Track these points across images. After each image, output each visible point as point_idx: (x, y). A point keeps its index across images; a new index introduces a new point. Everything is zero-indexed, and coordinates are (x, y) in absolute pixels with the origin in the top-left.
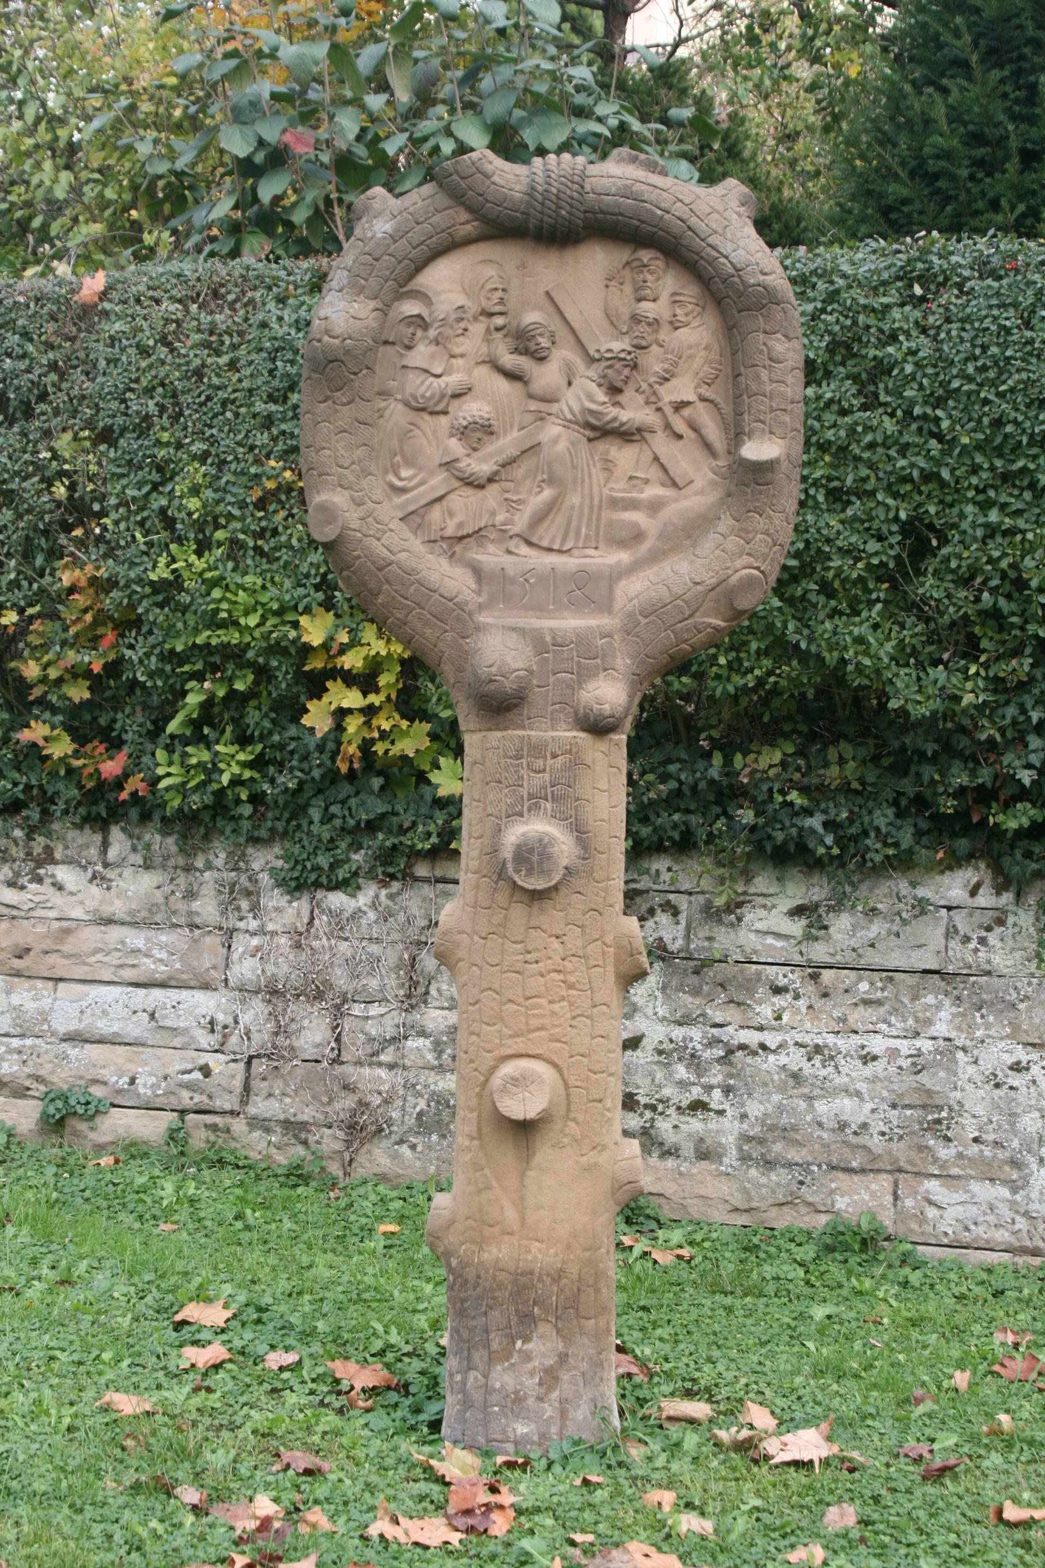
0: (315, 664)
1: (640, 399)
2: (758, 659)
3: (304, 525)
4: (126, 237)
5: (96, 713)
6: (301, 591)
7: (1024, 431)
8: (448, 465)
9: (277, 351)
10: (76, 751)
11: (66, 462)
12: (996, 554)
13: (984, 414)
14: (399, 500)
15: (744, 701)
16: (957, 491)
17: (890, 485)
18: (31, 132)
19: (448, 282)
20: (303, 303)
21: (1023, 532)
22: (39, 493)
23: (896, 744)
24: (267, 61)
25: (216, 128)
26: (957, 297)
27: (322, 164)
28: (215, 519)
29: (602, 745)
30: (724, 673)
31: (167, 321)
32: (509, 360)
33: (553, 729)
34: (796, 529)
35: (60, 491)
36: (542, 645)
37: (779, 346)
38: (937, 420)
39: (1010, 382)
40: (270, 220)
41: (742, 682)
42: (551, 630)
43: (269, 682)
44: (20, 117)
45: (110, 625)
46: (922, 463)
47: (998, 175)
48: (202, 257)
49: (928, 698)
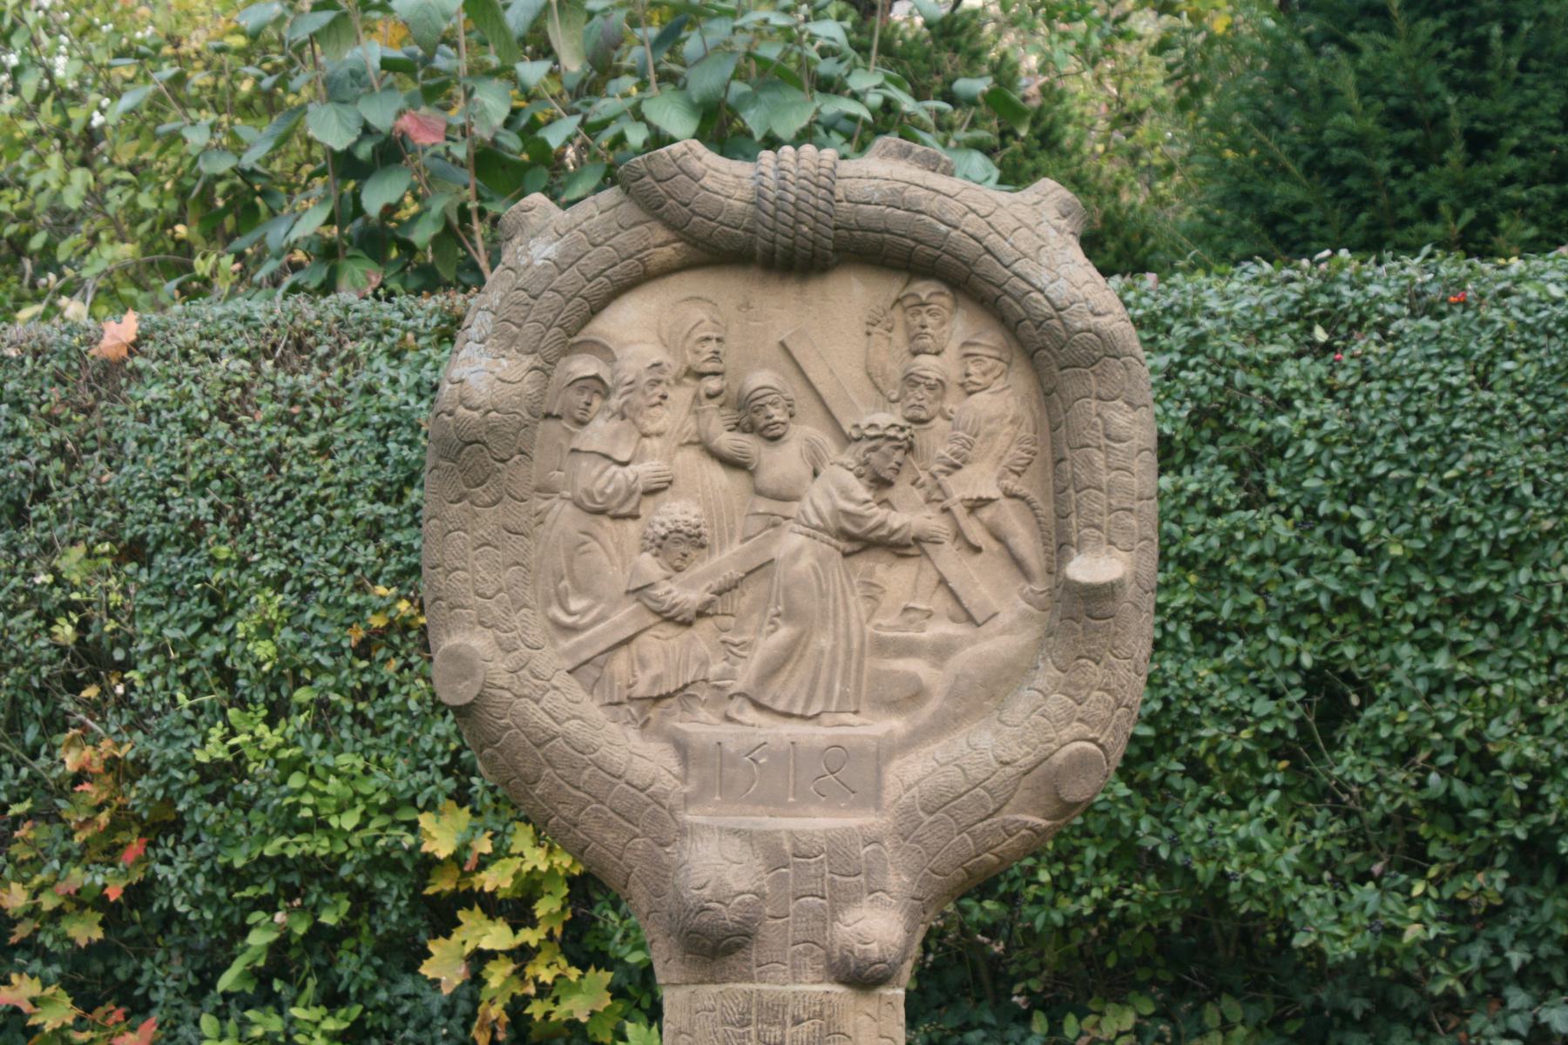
0: (442, 885)
1: (919, 495)
2: (1097, 874)
3: (428, 680)
4: (169, 263)
5: (113, 961)
6: (421, 776)
7: (1483, 536)
8: (638, 592)
9: (389, 427)
10: (79, 1019)
11: (74, 588)
12: (1447, 717)
13: (1424, 512)
14: (567, 643)
15: (1078, 936)
16: (1386, 624)
17: (1286, 617)
18: (31, 112)
19: (637, 329)
20: (427, 359)
21: (1487, 684)
22: (33, 635)
23: (1307, 1001)
24: (376, 15)
25: (302, 109)
26: (1379, 344)
27: (455, 161)
28: (296, 671)
29: (869, 1004)
30: (1047, 894)
31: (228, 385)
32: (727, 441)
33: (795, 980)
34: (1149, 683)
35: (65, 631)
36: (778, 856)
37: (1120, 417)
38: (1353, 522)
39: (1461, 466)
40: (378, 240)
41: (1073, 908)
42: (791, 833)
43: (372, 911)
44: (15, 91)
45: (136, 830)
46: (1333, 583)
47: (1434, 169)
48: (280, 292)
49: (1353, 931)
